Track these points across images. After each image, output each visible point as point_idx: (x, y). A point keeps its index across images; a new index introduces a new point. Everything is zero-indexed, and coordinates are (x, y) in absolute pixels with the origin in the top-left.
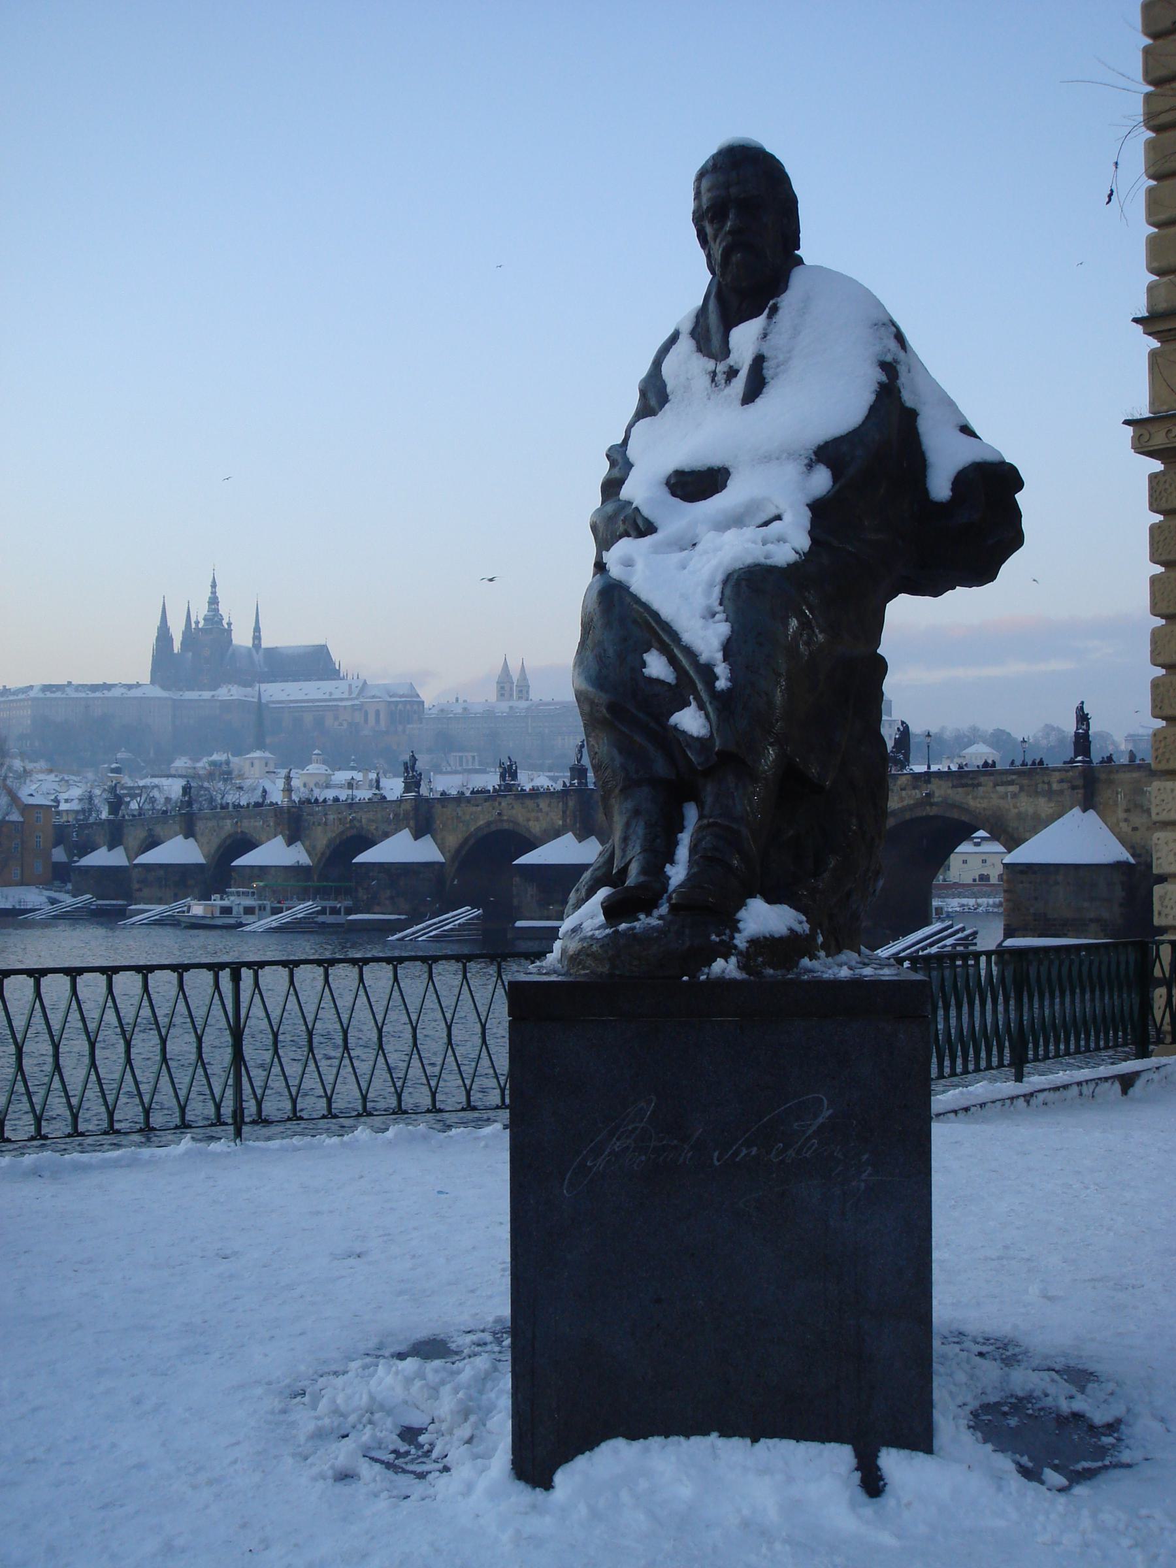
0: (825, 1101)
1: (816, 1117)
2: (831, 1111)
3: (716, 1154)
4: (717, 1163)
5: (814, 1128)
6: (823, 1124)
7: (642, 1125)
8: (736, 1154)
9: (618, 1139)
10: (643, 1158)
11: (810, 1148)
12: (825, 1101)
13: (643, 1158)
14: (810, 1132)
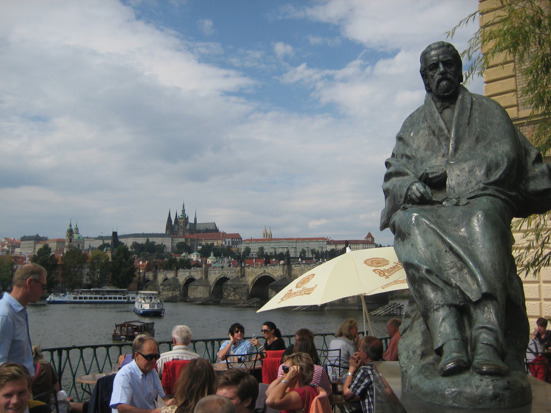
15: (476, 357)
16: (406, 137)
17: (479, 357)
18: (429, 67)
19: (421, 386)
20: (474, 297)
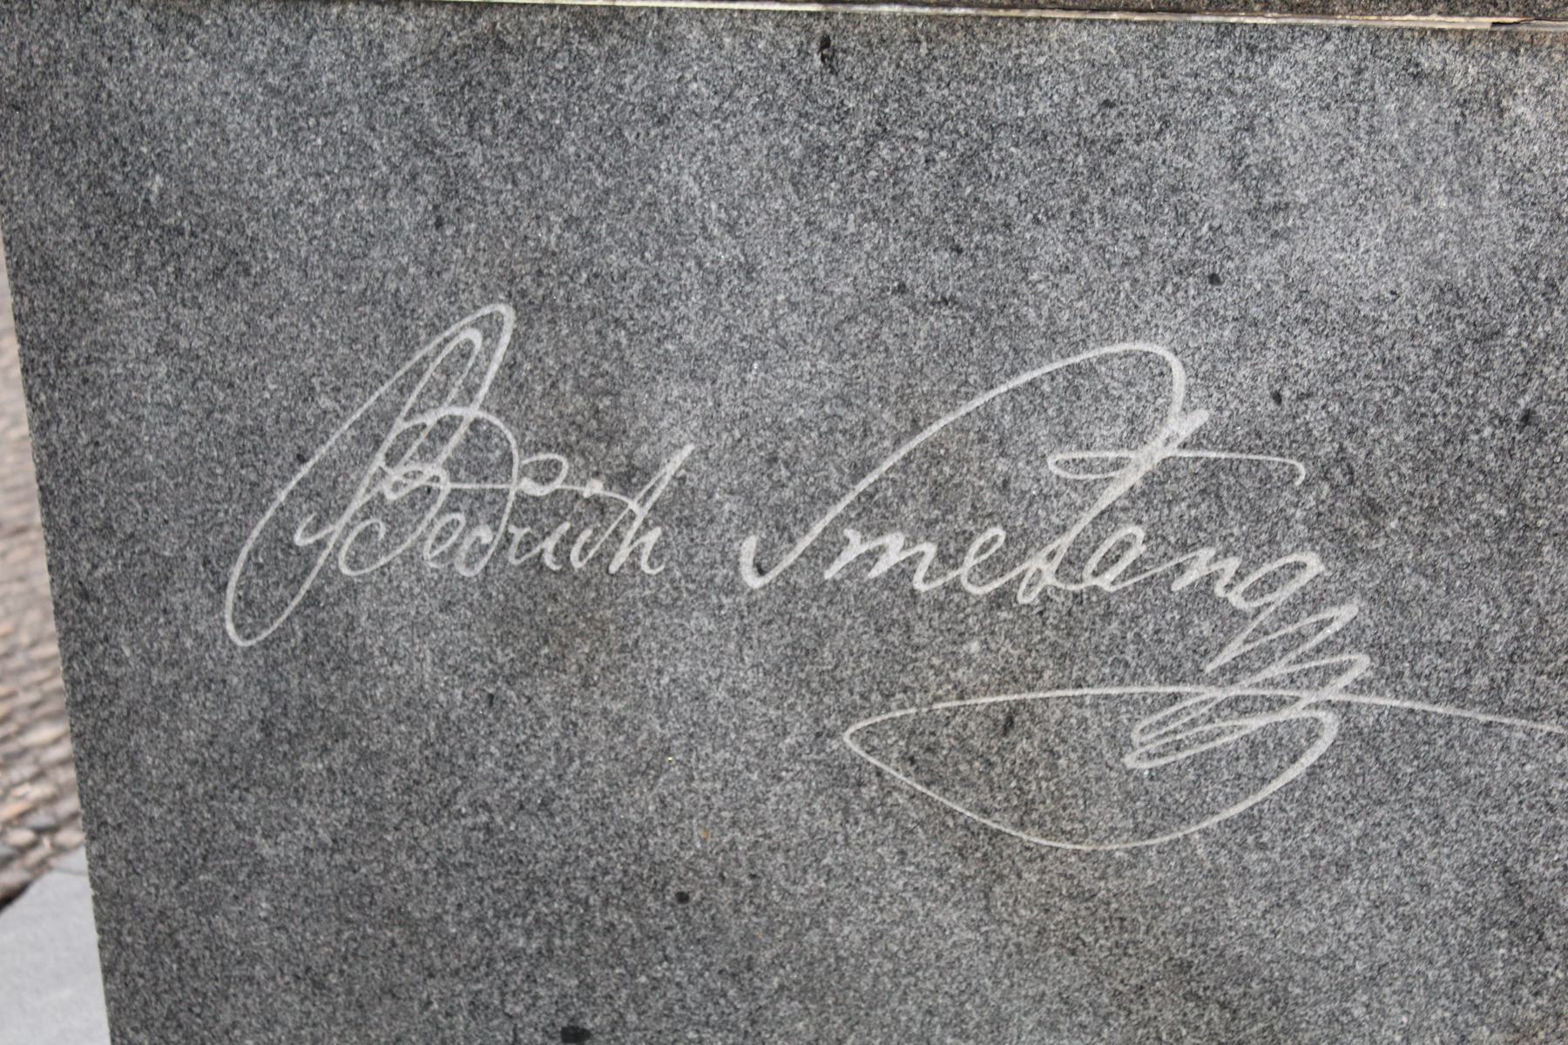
0: (1179, 375)
1: (1137, 432)
2: (1201, 417)
3: (749, 546)
4: (753, 581)
5: (1132, 478)
6: (1168, 468)
7: (472, 412)
8: (826, 550)
9: (392, 459)
11: (1109, 561)
12: (1179, 375)
13: (485, 534)
14: (1111, 495)
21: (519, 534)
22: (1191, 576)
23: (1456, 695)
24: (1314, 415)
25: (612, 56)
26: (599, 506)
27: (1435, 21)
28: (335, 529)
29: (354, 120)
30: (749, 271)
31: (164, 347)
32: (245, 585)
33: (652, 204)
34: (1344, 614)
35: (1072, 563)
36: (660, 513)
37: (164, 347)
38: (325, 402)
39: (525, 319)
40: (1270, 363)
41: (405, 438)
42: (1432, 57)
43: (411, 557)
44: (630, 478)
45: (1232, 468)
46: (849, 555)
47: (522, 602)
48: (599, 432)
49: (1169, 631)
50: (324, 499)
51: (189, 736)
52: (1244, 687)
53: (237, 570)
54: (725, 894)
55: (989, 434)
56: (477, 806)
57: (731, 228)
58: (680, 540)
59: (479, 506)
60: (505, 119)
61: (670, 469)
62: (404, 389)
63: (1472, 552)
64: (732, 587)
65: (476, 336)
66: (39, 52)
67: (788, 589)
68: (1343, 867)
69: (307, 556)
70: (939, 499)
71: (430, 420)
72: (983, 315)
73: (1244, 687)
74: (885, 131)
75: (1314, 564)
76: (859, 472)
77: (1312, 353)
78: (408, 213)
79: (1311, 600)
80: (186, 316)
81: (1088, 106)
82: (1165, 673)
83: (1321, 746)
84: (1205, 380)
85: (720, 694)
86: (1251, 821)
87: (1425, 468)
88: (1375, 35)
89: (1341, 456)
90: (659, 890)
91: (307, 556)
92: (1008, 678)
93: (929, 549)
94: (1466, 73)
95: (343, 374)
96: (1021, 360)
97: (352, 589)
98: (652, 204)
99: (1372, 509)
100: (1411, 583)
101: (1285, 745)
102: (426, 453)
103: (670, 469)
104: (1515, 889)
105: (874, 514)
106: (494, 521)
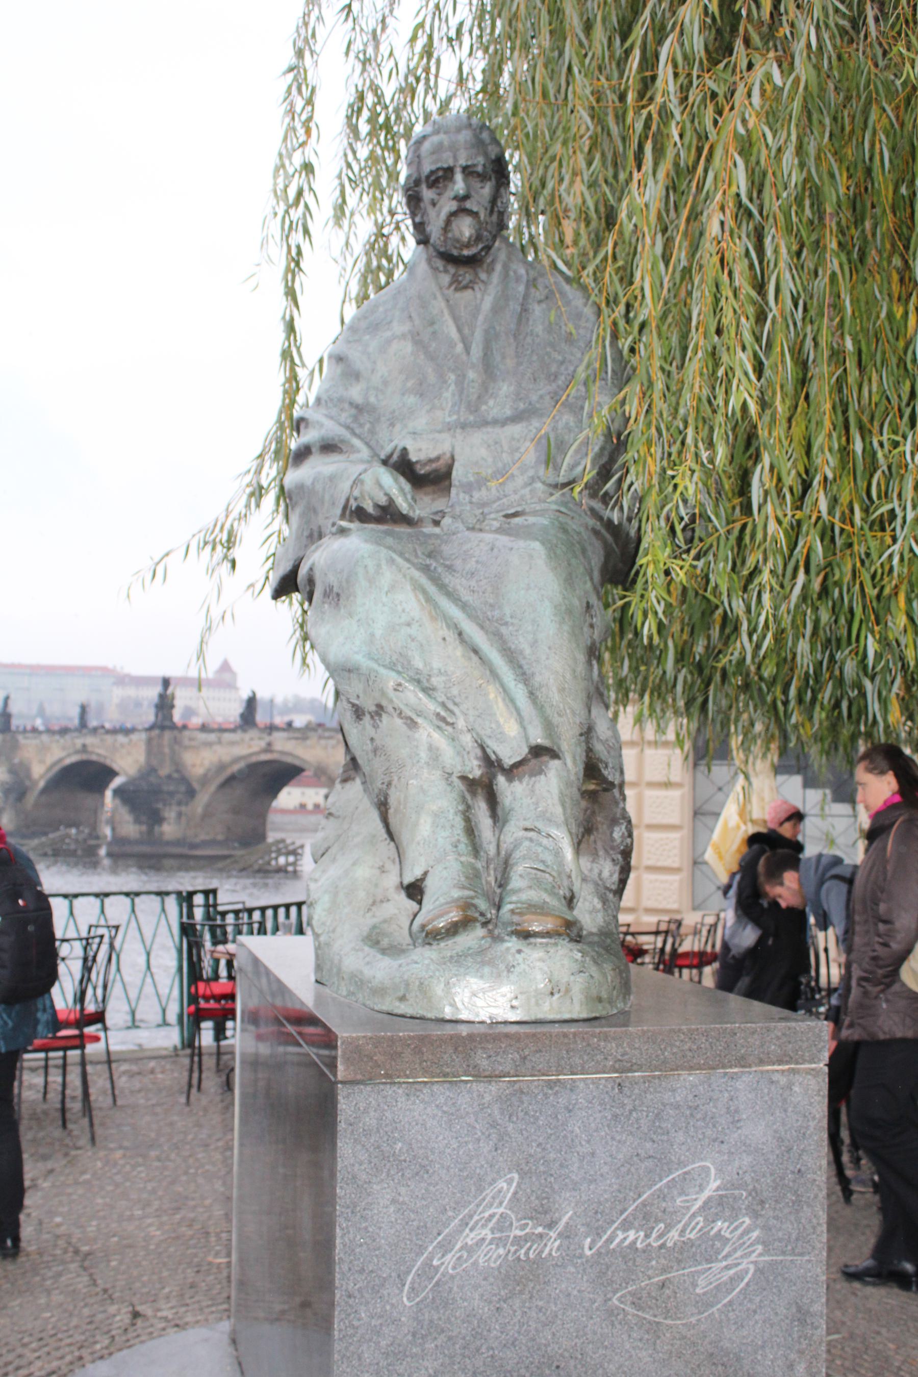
0: (713, 1171)
1: (702, 1188)
2: (718, 1183)
4: (588, 1253)
5: (699, 1203)
6: (710, 1199)
7: (501, 1210)
8: (610, 1240)
9: (471, 1230)
10: (501, 1251)
12: (713, 1171)
15: (508, 899)
16: (355, 355)
17: (514, 898)
18: (428, 177)
19: (368, 972)
20: (509, 754)
21: (513, 1249)
22: (715, 1230)
23: (784, 1253)
24: (747, 1178)
25: (556, 1094)
26: (541, 1236)
27: (776, 1067)
28: (449, 1256)
29: (471, 1120)
30: (593, 1154)
31: (393, 1201)
32: (413, 1283)
33: (565, 1137)
34: (755, 1234)
35: (683, 1231)
36: (560, 1235)
37: (393, 1201)
38: (450, 1213)
39: (521, 1178)
40: (737, 1164)
41: (477, 1223)
42: (776, 1077)
43: (475, 1263)
44: (551, 1225)
45: (726, 1196)
46: (617, 1240)
47: (512, 1273)
48: (543, 1213)
49: (706, 1250)
50: (445, 1247)
51: (383, 1343)
52: (729, 1261)
53: (410, 1278)
54: (572, 1362)
55: (661, 1196)
56: (489, 1349)
57: (588, 1142)
58: (566, 1242)
59: (499, 1242)
60: (521, 1115)
61: (565, 1219)
62: (478, 1206)
63: (786, 1210)
64: (581, 1256)
65: (505, 1185)
66: (362, 1106)
67: (599, 1253)
68: (755, 1312)
69: (437, 1269)
70: (646, 1218)
71: (486, 1214)
72: (660, 1160)
73: (729, 1261)
74: (635, 1109)
75: (747, 1221)
76: (622, 1212)
77: (747, 1160)
78: (486, 1147)
79: (747, 1231)
80: (403, 1190)
81: (690, 1097)
82: (709, 1261)
83: (749, 1275)
84: (720, 1170)
85: (575, 1292)
86: (730, 1303)
87: (775, 1188)
88: (762, 1072)
89: (755, 1189)
90: (550, 1367)
91: (437, 1269)
92: (664, 1270)
93: (642, 1234)
94: (783, 1080)
95: (457, 1203)
96: (670, 1172)
97: (452, 1277)
98: (565, 1137)
99: (762, 1202)
100: (772, 1222)
101: (739, 1277)
102: (484, 1226)
103: (565, 1219)
104: (799, 1309)
105: (626, 1226)
106: (505, 1246)
